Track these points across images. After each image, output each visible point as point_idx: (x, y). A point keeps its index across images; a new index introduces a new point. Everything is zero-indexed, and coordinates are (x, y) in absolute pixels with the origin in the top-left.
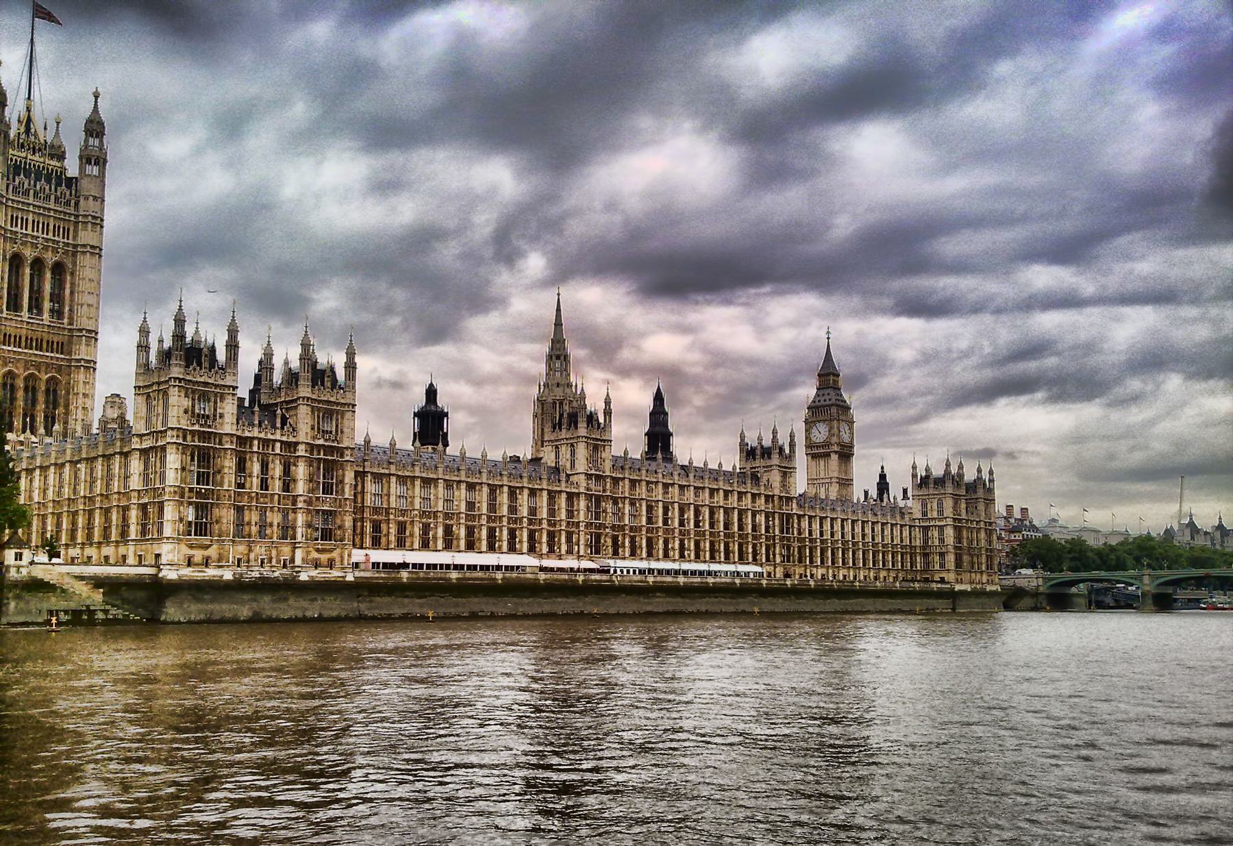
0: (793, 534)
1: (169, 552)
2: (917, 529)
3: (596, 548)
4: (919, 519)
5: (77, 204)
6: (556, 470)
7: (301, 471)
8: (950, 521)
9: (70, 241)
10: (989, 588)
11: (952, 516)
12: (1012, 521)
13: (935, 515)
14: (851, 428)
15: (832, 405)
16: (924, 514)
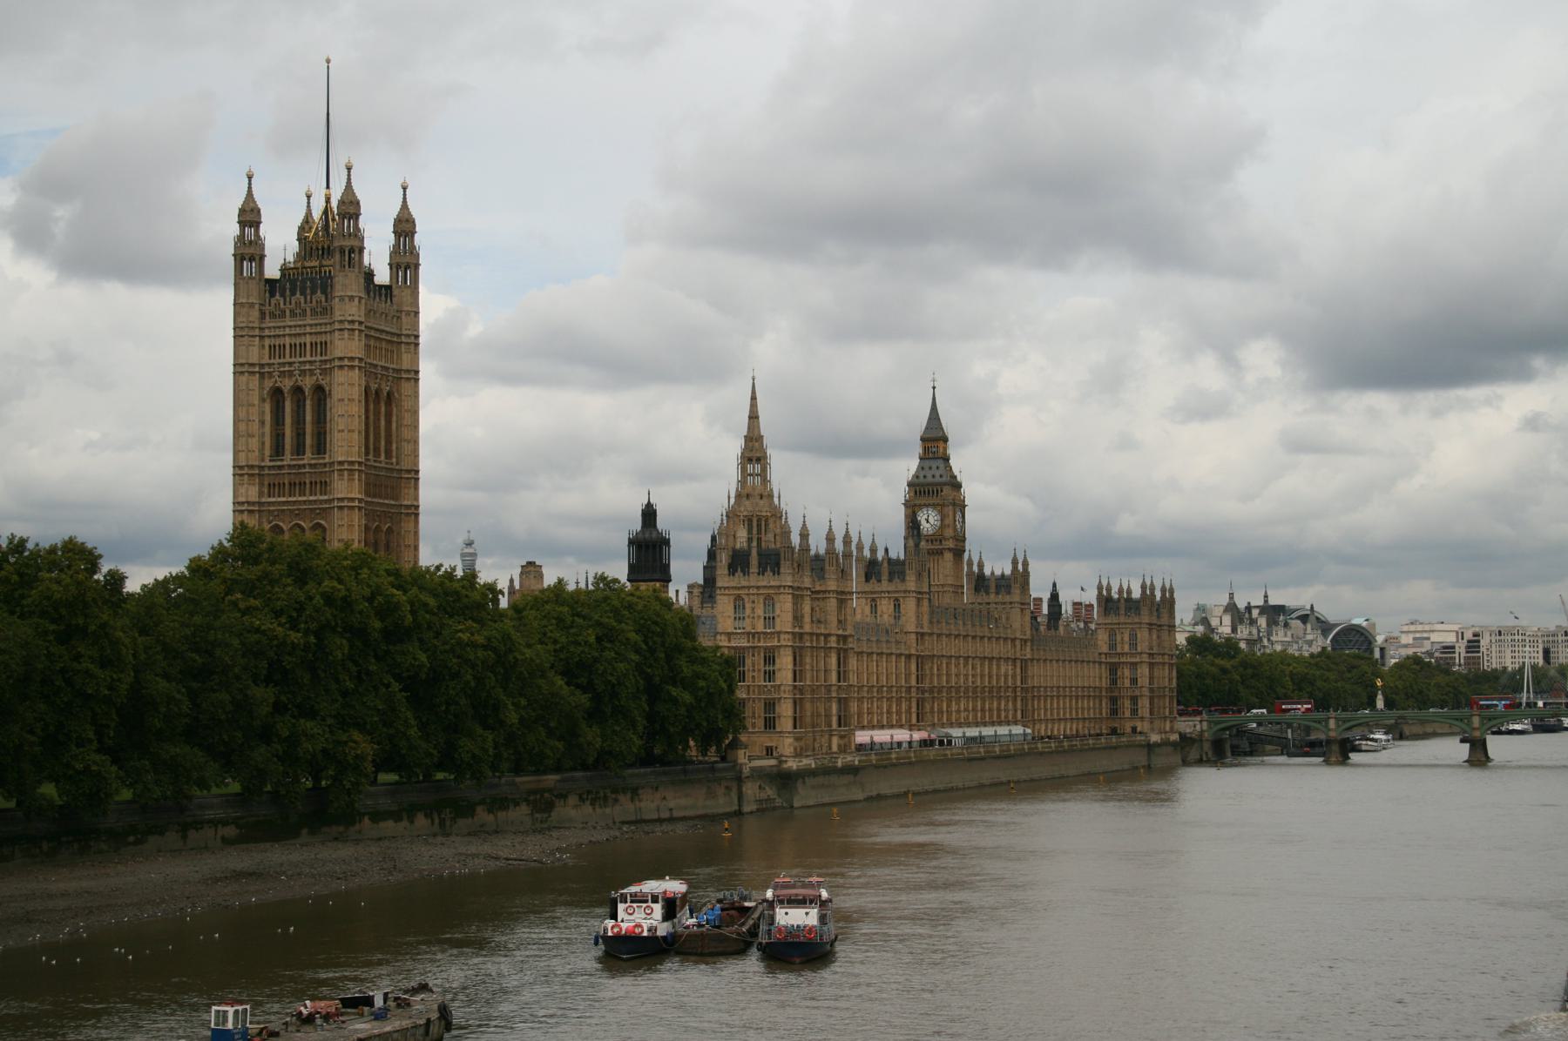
1: (787, 746)
4: (1106, 654)
8: (1145, 658)
13: (1126, 649)
15: (945, 484)
16: (1112, 646)
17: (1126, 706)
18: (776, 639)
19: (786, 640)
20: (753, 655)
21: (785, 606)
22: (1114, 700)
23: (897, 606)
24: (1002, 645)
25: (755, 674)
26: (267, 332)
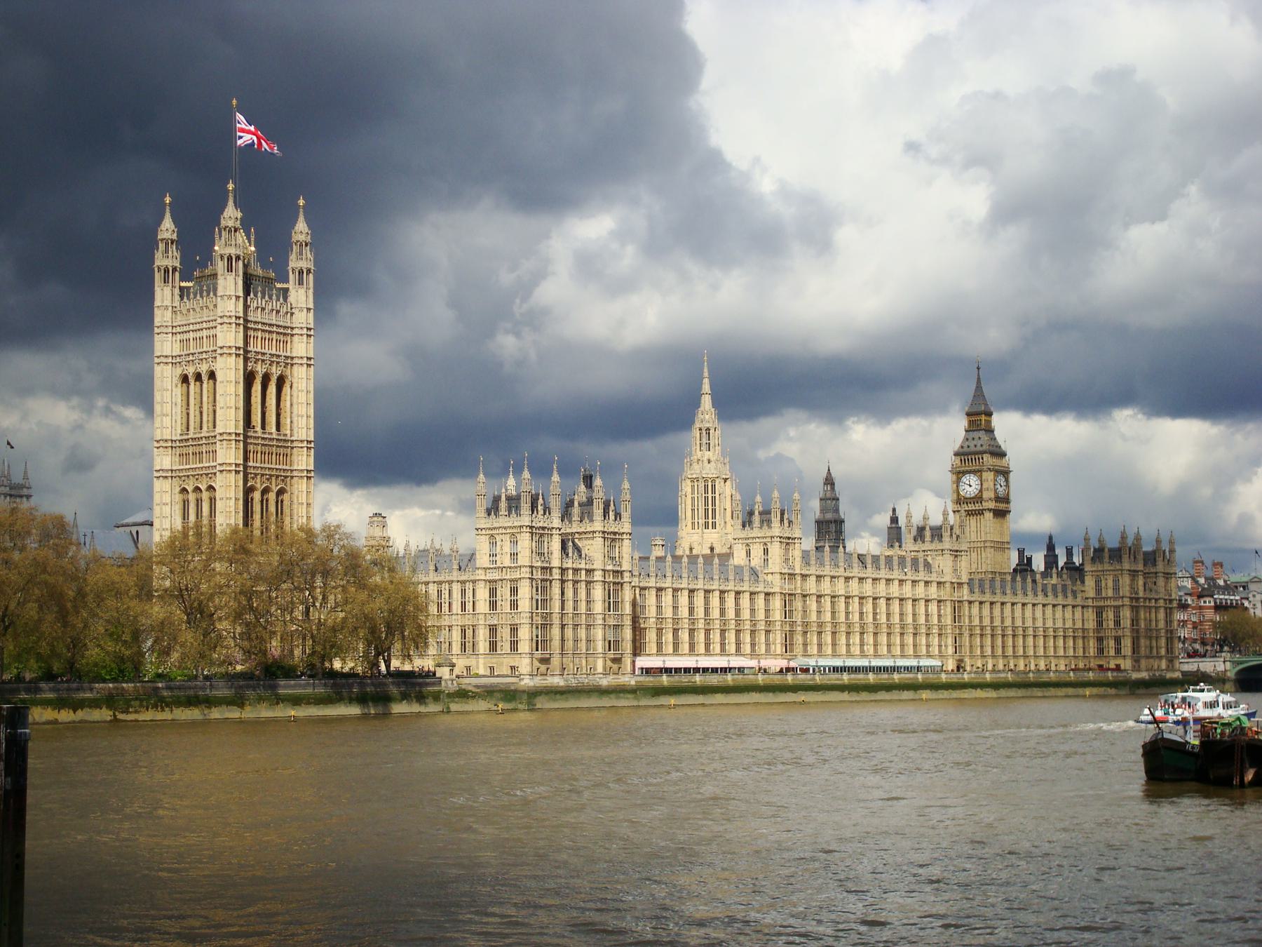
0: (964, 623)
2: (1090, 610)
3: (788, 646)
4: (1093, 598)
5: (292, 314)
6: (754, 572)
8: (1127, 601)
9: (288, 354)
11: (1128, 595)
12: (1202, 581)
13: (1110, 593)
14: (1007, 481)
15: (985, 452)
17: (1110, 646)
18: (518, 572)
19: (525, 573)
20: (502, 587)
21: (525, 541)
22: (1100, 640)
23: (766, 551)
24: (799, 582)
25: (503, 603)
26: (178, 329)
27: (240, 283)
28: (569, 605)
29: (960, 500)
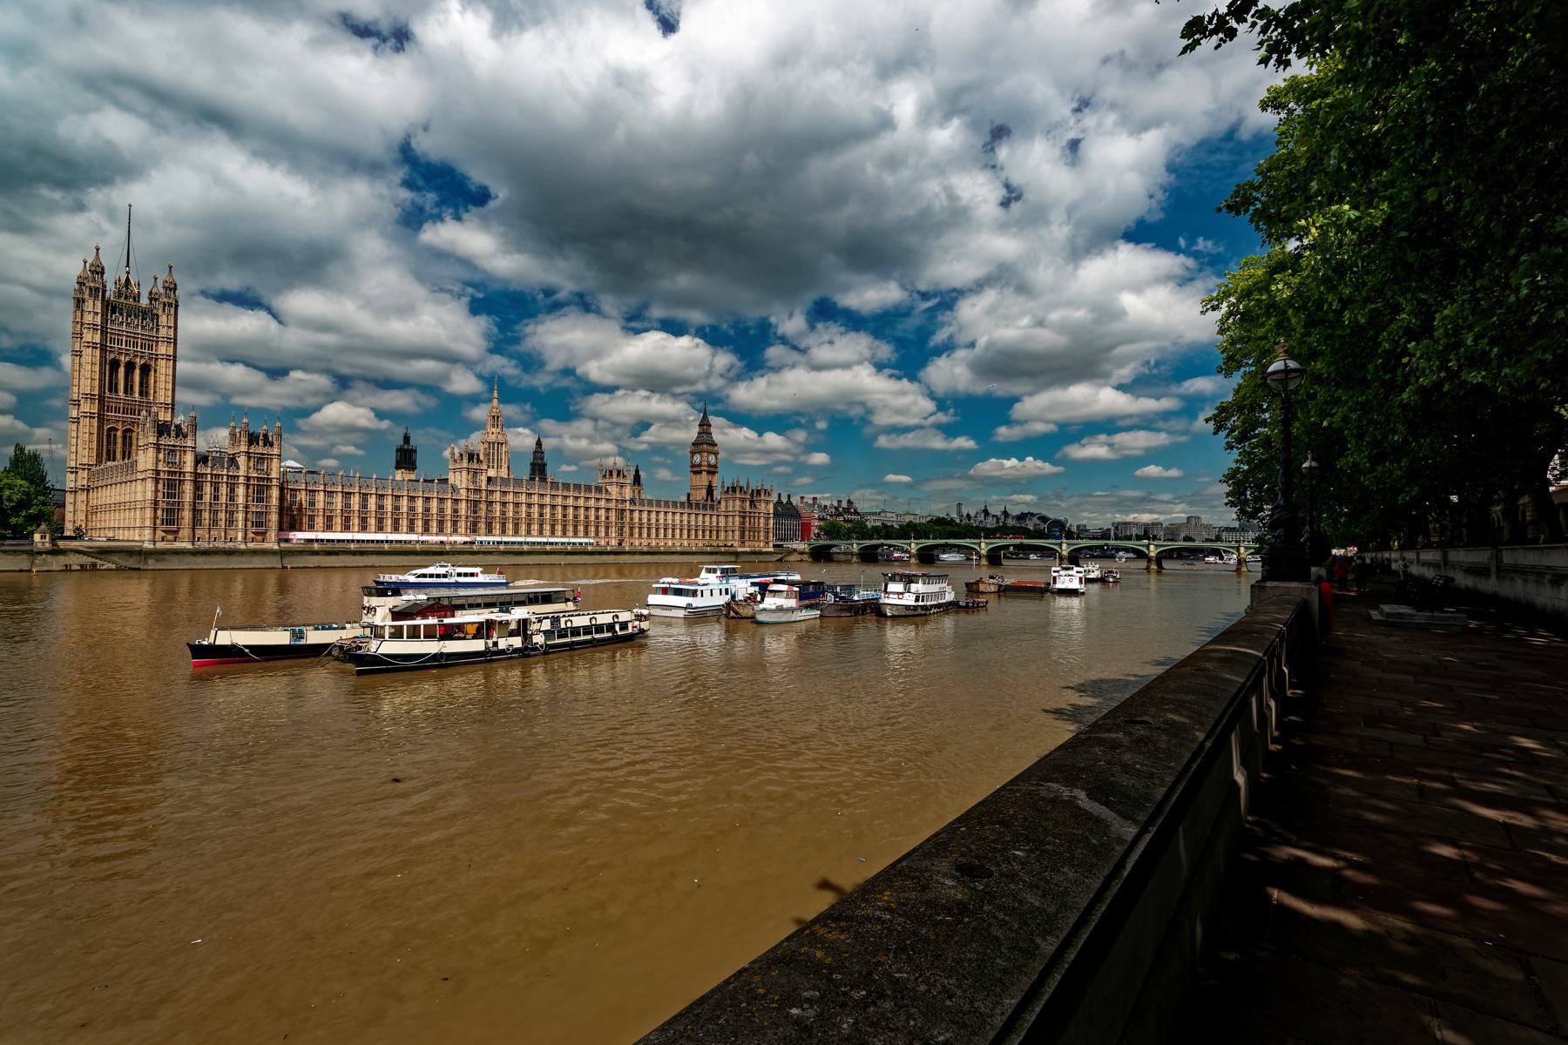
7: (241, 491)
10: (764, 550)
27: (99, 304)
28: (207, 498)
29: (693, 466)
